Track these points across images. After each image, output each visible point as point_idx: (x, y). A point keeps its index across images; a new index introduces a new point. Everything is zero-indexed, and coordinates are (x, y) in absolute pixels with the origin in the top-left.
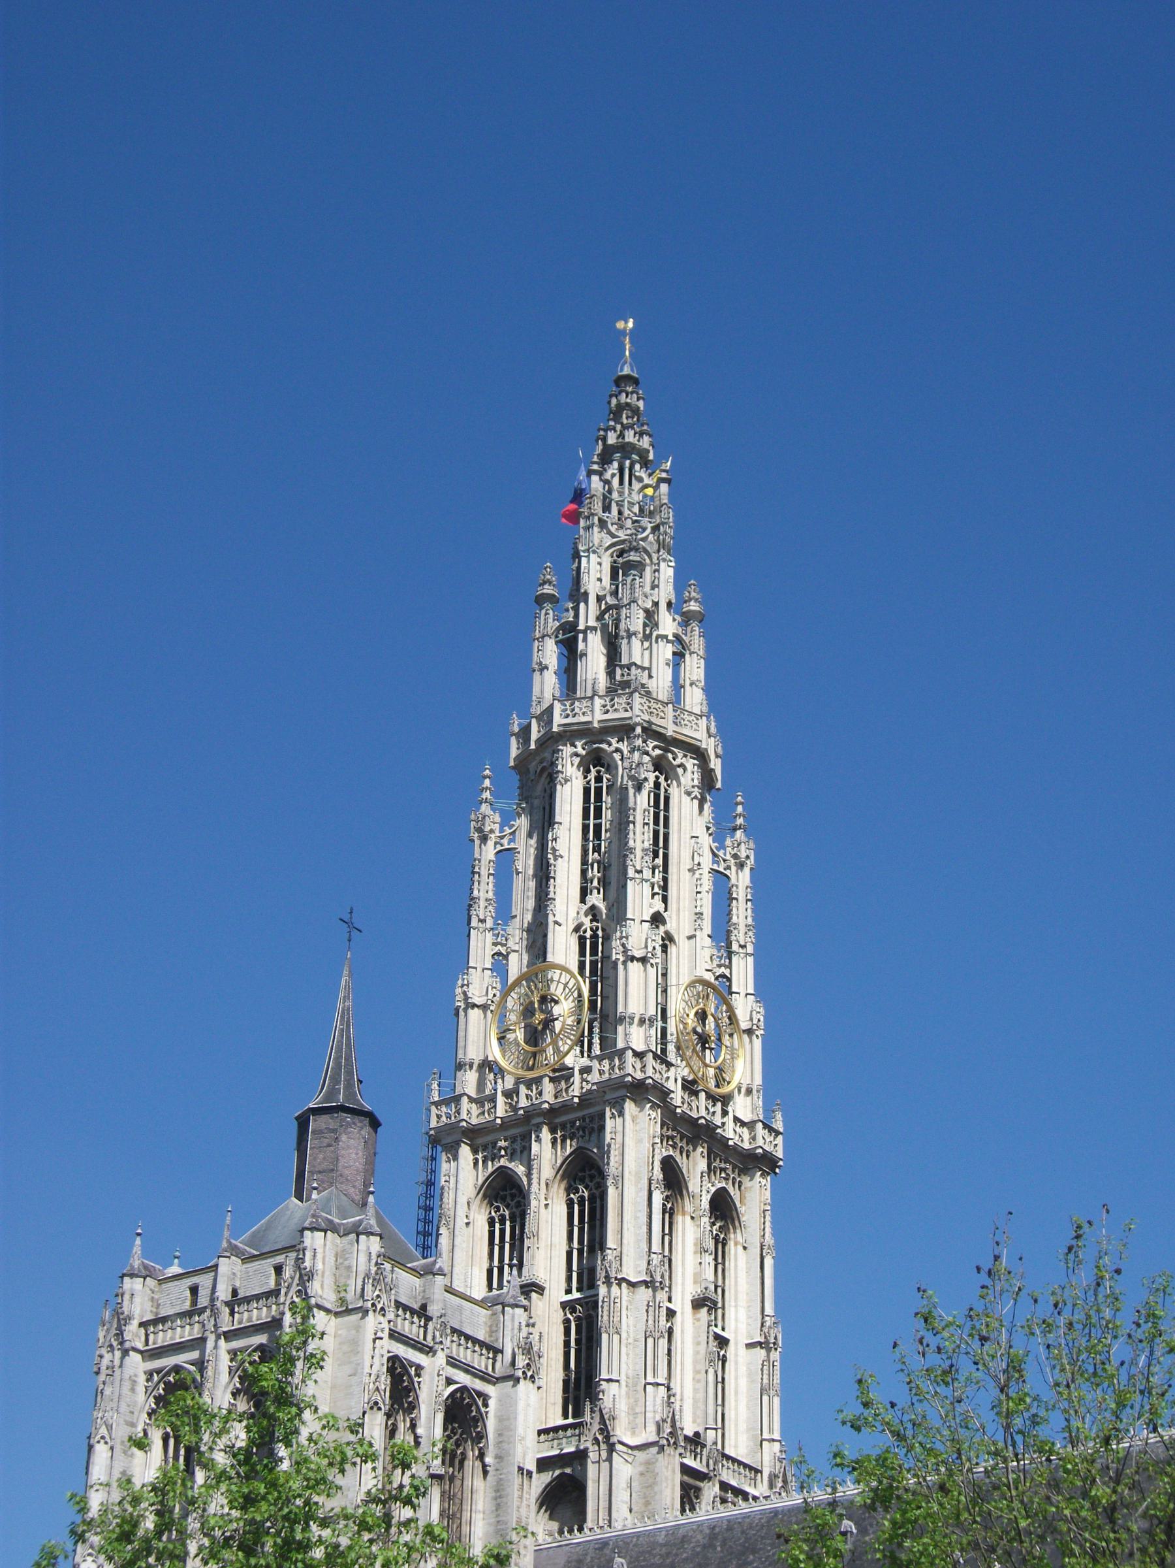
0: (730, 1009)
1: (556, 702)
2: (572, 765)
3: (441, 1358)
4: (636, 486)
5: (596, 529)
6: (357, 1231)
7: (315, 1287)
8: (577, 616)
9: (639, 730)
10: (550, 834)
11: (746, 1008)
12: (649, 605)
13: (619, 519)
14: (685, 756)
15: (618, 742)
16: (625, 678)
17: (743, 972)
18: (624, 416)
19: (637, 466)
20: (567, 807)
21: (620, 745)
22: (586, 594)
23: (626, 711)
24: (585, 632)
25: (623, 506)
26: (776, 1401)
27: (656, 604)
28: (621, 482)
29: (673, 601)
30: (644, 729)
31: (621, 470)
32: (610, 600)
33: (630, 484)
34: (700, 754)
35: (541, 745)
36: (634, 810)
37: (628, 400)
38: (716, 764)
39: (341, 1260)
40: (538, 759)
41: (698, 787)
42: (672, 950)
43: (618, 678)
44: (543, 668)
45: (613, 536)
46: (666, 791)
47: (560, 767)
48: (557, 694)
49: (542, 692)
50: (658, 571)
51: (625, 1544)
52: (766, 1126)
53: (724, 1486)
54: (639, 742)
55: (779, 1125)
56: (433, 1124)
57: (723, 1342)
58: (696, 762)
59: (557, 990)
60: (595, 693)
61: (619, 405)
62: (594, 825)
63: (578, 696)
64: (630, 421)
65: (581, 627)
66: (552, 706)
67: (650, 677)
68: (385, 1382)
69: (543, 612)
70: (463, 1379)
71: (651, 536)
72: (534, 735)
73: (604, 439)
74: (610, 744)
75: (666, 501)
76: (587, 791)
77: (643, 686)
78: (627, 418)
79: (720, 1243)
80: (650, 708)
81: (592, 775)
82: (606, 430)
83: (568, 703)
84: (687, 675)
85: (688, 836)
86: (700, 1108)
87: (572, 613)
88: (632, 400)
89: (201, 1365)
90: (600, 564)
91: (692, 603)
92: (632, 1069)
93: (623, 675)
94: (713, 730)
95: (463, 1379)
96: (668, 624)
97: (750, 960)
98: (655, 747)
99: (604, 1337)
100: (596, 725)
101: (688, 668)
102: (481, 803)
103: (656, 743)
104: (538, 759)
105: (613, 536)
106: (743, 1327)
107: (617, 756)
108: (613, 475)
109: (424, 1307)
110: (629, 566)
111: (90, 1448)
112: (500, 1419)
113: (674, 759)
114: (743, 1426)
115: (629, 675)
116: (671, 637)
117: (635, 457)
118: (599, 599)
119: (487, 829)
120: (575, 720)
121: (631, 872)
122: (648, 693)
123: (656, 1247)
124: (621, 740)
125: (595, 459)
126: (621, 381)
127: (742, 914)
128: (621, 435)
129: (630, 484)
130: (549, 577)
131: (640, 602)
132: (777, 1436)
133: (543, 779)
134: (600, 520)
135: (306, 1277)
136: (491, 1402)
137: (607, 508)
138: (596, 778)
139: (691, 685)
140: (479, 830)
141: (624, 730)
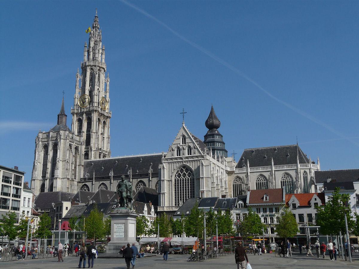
3: (74, 143)
6: (66, 130)
7: (61, 137)
11: (108, 99)
12: (98, 49)
17: (108, 95)
26: (109, 144)
31: (95, 29)
38: (105, 69)
39: (64, 135)
42: (100, 93)
51: (93, 162)
55: (111, 113)
56: (71, 112)
57: (104, 138)
59: (86, 97)
68: (69, 147)
70: (76, 145)
76: (90, 73)
79: (104, 127)
81: (91, 71)
86: (103, 112)
89: (48, 143)
92: (95, 109)
95: (76, 145)
96: (101, 51)
99: (91, 138)
106: (106, 136)
109: (72, 138)
110: (96, 44)
111: (35, 152)
112: (80, 149)
114: (106, 147)
121: (95, 85)
123: (97, 128)
126: (95, 17)
127: (108, 88)
128: (96, 25)
132: (109, 148)
135: (60, 136)
140: (77, 76)
141: (95, 66)
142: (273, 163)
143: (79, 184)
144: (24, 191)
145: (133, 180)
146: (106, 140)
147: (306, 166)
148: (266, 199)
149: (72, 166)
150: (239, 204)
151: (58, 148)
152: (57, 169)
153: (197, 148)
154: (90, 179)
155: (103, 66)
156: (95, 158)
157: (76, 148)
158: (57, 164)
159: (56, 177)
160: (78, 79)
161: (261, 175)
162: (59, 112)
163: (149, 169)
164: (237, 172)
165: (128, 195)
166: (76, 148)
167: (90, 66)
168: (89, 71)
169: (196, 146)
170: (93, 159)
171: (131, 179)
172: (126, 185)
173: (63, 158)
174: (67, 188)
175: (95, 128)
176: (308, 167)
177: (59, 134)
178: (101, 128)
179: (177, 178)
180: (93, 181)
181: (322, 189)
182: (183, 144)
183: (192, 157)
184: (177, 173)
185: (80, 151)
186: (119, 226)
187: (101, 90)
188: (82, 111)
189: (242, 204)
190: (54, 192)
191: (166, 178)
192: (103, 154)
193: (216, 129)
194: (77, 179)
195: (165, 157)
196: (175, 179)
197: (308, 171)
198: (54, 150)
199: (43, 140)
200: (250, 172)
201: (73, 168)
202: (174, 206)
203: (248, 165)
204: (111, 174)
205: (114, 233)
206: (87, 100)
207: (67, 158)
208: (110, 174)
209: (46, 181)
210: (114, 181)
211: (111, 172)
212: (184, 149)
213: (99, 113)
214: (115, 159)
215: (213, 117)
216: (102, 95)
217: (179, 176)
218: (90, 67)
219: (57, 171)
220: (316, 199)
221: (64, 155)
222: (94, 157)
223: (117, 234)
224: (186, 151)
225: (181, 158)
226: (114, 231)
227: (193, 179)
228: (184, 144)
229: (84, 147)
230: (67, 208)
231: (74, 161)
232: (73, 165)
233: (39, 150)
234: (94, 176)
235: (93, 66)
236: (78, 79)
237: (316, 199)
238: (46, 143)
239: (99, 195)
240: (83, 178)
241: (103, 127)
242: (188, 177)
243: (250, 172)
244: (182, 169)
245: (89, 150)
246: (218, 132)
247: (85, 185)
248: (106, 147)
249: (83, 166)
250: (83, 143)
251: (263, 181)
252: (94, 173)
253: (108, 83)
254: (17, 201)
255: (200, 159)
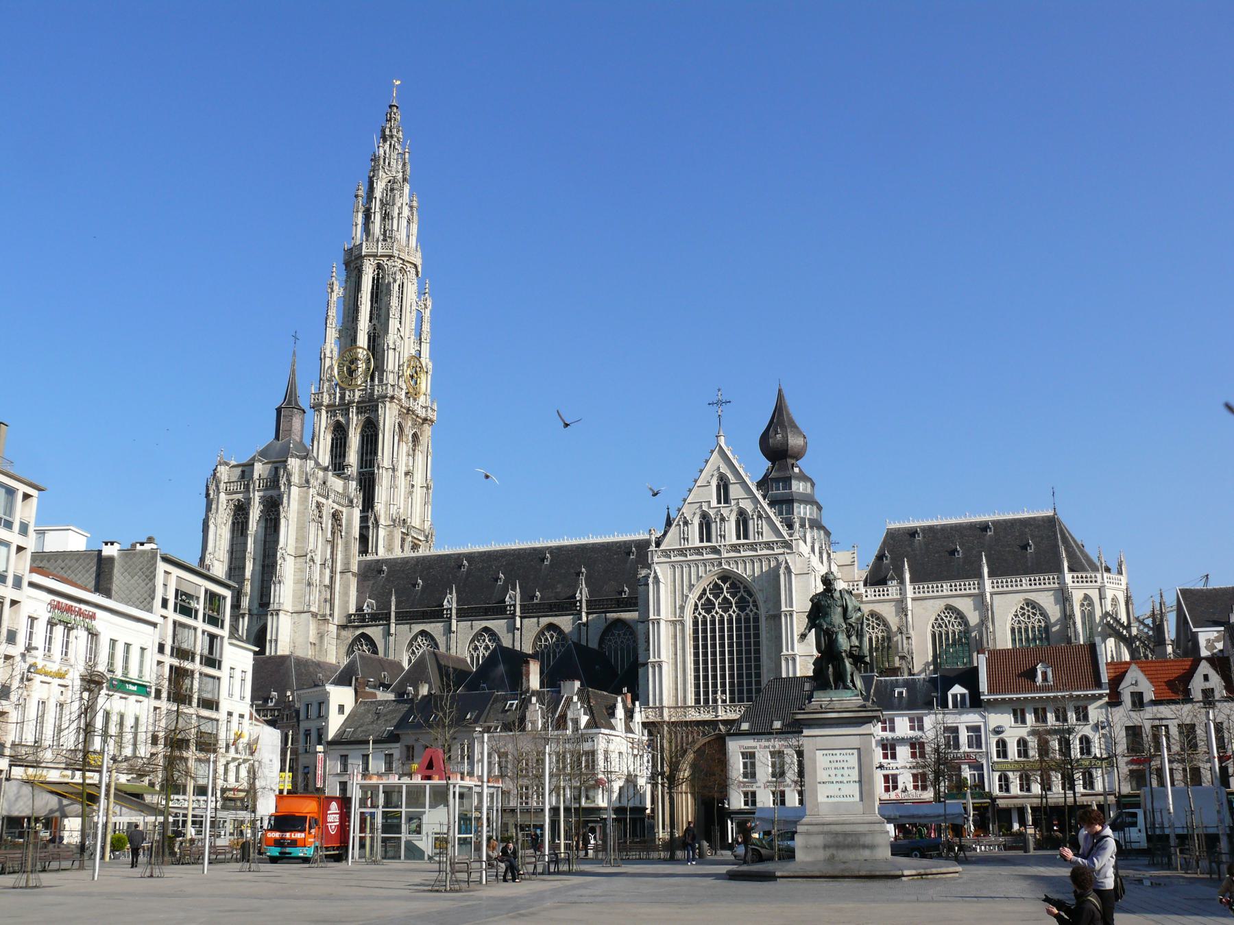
0: (420, 362)
3: (330, 501)
12: (400, 205)
17: (426, 349)
26: (430, 507)
31: (390, 145)
34: (416, 266)
39: (302, 469)
52: (431, 408)
53: (413, 537)
70: (336, 506)
76: (373, 278)
81: (376, 272)
89: (249, 500)
95: (336, 506)
97: (428, 345)
107: (386, 267)
112: (347, 520)
114: (418, 515)
121: (391, 315)
126: (391, 106)
127: (426, 327)
132: (429, 519)
135: (289, 475)
136: (344, 514)
141: (390, 257)
142: (986, 570)
143: (344, 633)
144: (231, 644)
145: (526, 621)
146: (419, 493)
147: (1089, 580)
148: (1045, 678)
149: (322, 574)
150: (955, 696)
151: (282, 515)
152: (280, 582)
153: (768, 517)
154: (380, 617)
155: (412, 259)
156: (390, 549)
157: (336, 516)
158: (278, 567)
159: (276, 607)
160: (335, 297)
161: (949, 608)
162: (279, 401)
163: (575, 586)
164: (869, 598)
165: (852, 644)
166: (336, 516)
167: (375, 256)
169: (764, 510)
170: (382, 553)
171: (518, 620)
172: (845, 609)
173: (296, 548)
174: (311, 643)
175: (389, 454)
176: (1096, 582)
177: (285, 467)
178: (404, 454)
179: (700, 614)
180: (389, 625)
181: (1216, 644)
182: (719, 502)
183: (753, 547)
184: (700, 598)
185: (347, 525)
186: (835, 758)
187: (407, 336)
188: (347, 398)
189: (963, 696)
190: (270, 658)
191: (666, 612)
192: (410, 539)
193: (793, 461)
194: (338, 618)
195: (658, 545)
196: (695, 617)
197: (1094, 594)
198: (266, 520)
199: (232, 487)
200: (913, 599)
201: (327, 582)
202: (693, 704)
203: (907, 576)
204: (451, 602)
205: (819, 785)
206: (362, 366)
207: (310, 548)
208: (445, 602)
209: (241, 619)
210: (461, 624)
211: (449, 596)
212: (723, 519)
213: (402, 407)
214: (460, 555)
215: (786, 424)
216: (409, 350)
217: (709, 606)
219: (277, 588)
220: (1206, 678)
221: (302, 537)
222: (387, 547)
223: (832, 789)
224: (731, 527)
225: (715, 550)
226: (819, 780)
227: (756, 619)
228: (723, 505)
229: (357, 513)
230: (341, 709)
231: (328, 557)
232: (328, 571)
233: (219, 521)
234: (393, 608)
235: (382, 256)
236: (335, 299)
237: (1206, 678)
238: (240, 496)
239: (426, 667)
240: (355, 615)
241: (411, 452)
242: (704, 614)
243: (913, 599)
244: (716, 585)
245: (370, 524)
246: (800, 470)
247: (363, 635)
248: (419, 515)
249: (354, 574)
250: (355, 501)
251: (953, 626)
252: (393, 598)
253: (428, 311)
254: (213, 677)
255: (781, 551)
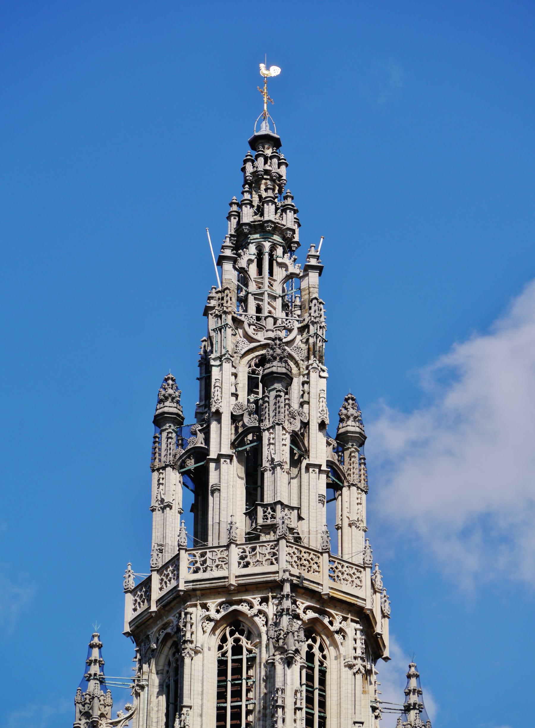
1: (182, 552)
2: (204, 632)
4: (279, 274)
5: (229, 331)
8: (207, 440)
9: (287, 589)
10: (177, 721)
12: (297, 426)
13: (258, 319)
14: (345, 619)
15: (260, 604)
16: (269, 522)
18: (263, 187)
19: (280, 251)
20: (197, 687)
21: (264, 607)
22: (218, 415)
23: (272, 563)
24: (217, 461)
25: (262, 300)
27: (305, 425)
28: (260, 272)
29: (327, 422)
30: (294, 587)
32: (249, 421)
33: (271, 273)
35: (164, 606)
36: (283, 691)
37: (267, 167)
40: (160, 624)
41: (362, 659)
43: (260, 521)
44: (166, 506)
45: (251, 340)
46: (322, 663)
47: (188, 635)
48: (185, 542)
49: (164, 537)
50: (308, 383)
54: (287, 604)
58: (358, 626)
60: (232, 542)
61: (254, 174)
62: (232, 707)
63: (210, 545)
64: (270, 193)
65: (213, 455)
66: (177, 557)
67: (300, 518)
69: (164, 434)
71: (299, 338)
72: (156, 594)
73: (239, 215)
74: (251, 607)
75: (316, 295)
76: (222, 663)
77: (291, 530)
78: (266, 190)
80: (300, 559)
81: (230, 642)
82: (240, 206)
83: (198, 553)
84: (345, 514)
85: (351, 722)
87: (201, 436)
88: (273, 166)
90: (235, 375)
91: (350, 422)
93: (265, 518)
94: (379, 584)
98: (307, 608)
100: (233, 581)
101: (346, 505)
102: (89, 680)
103: (308, 604)
104: (160, 624)
105: (251, 340)
107: (259, 621)
108: (250, 261)
113: (331, 623)
115: (273, 517)
116: (324, 468)
117: (277, 238)
118: (235, 419)
119: (96, 713)
120: (207, 575)
122: (298, 539)
124: (264, 600)
125: (228, 243)
128: (260, 211)
129: (271, 273)
130: (170, 391)
131: (286, 425)
133: (166, 650)
134: (234, 319)
137: (243, 301)
138: (233, 648)
139: (350, 525)
168: (215, 641)
218: (213, 603)
